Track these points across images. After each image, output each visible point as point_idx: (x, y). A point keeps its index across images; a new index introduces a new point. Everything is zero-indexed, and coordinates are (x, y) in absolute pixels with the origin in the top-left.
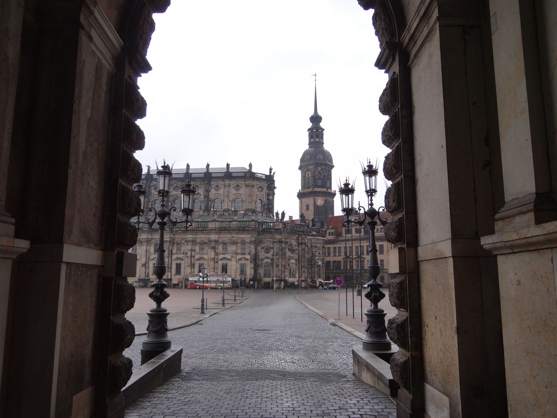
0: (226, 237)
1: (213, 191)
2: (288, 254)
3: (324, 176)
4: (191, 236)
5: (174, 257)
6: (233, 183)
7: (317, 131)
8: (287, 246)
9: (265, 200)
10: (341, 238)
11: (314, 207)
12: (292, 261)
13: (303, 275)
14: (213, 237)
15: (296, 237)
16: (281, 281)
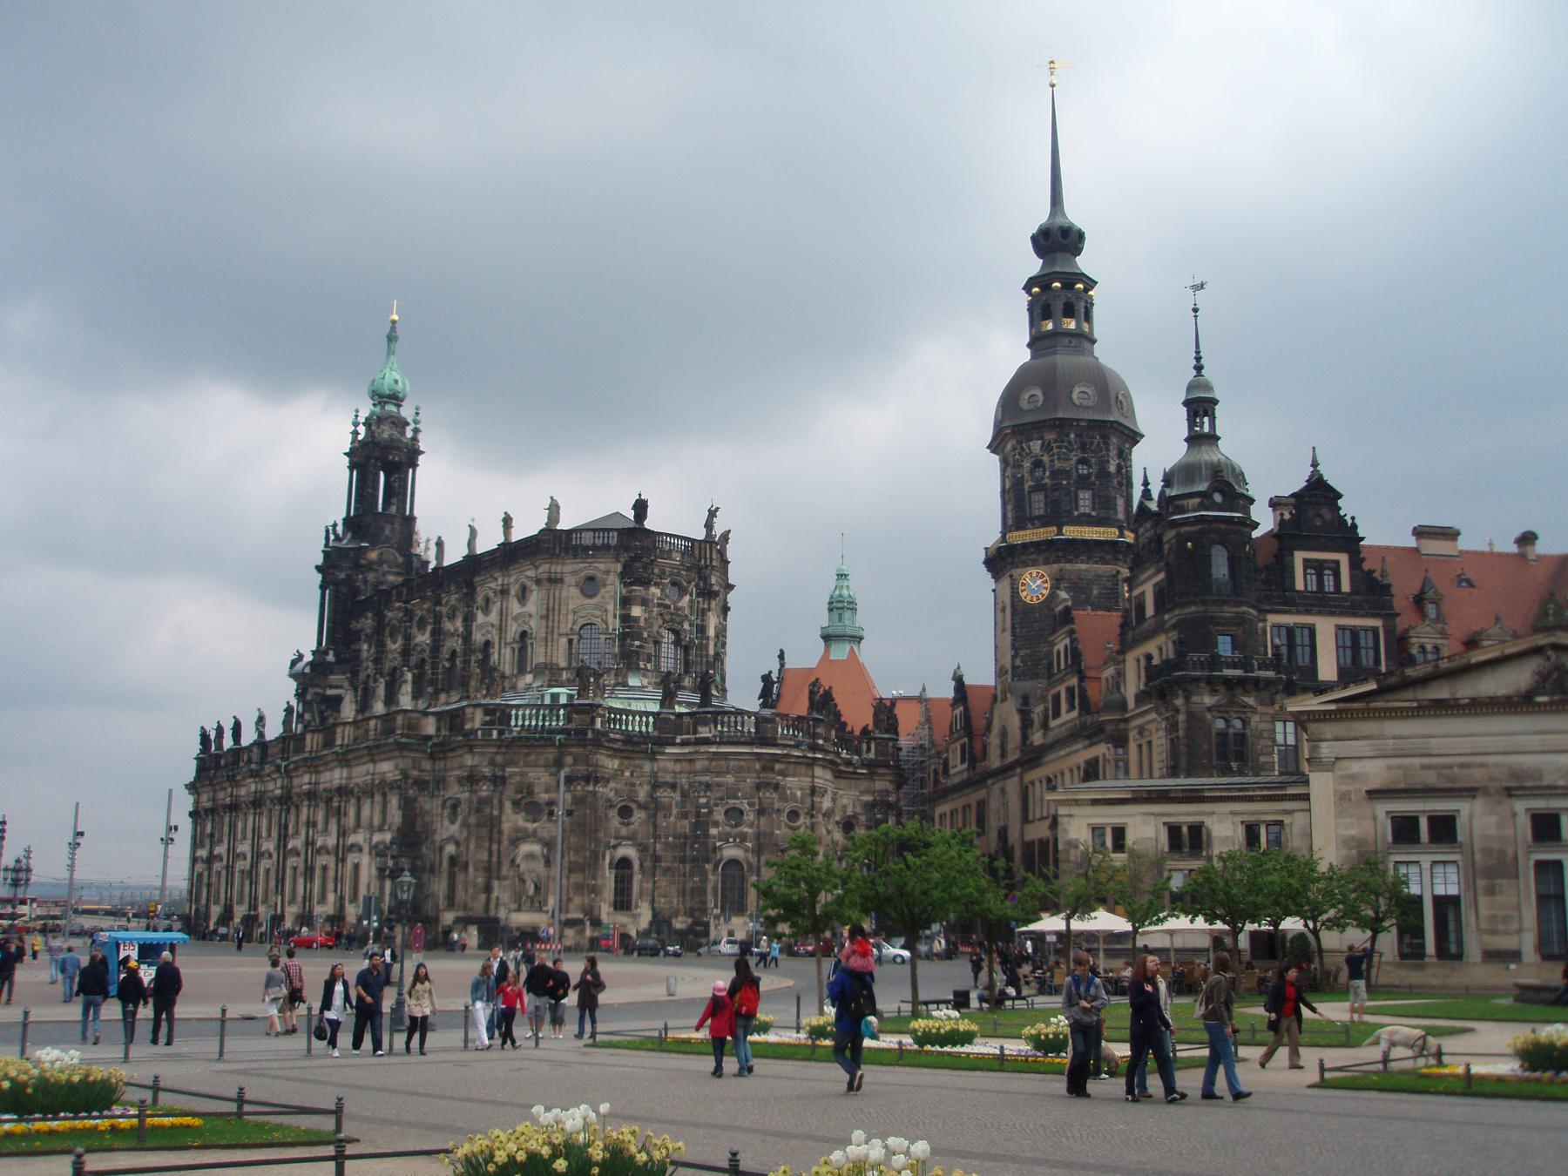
0: (361, 773)
1: (480, 618)
2: (512, 820)
3: (1055, 474)
4: (306, 778)
5: (290, 846)
6: (513, 579)
7: (1046, 287)
8: (510, 791)
9: (615, 624)
10: (1049, 740)
11: (1013, 614)
12: (525, 848)
13: (577, 900)
14: (335, 777)
15: (551, 754)
16: (464, 922)
